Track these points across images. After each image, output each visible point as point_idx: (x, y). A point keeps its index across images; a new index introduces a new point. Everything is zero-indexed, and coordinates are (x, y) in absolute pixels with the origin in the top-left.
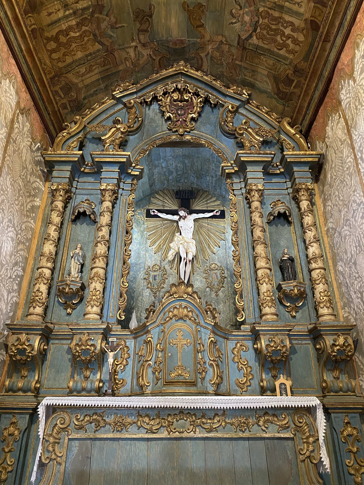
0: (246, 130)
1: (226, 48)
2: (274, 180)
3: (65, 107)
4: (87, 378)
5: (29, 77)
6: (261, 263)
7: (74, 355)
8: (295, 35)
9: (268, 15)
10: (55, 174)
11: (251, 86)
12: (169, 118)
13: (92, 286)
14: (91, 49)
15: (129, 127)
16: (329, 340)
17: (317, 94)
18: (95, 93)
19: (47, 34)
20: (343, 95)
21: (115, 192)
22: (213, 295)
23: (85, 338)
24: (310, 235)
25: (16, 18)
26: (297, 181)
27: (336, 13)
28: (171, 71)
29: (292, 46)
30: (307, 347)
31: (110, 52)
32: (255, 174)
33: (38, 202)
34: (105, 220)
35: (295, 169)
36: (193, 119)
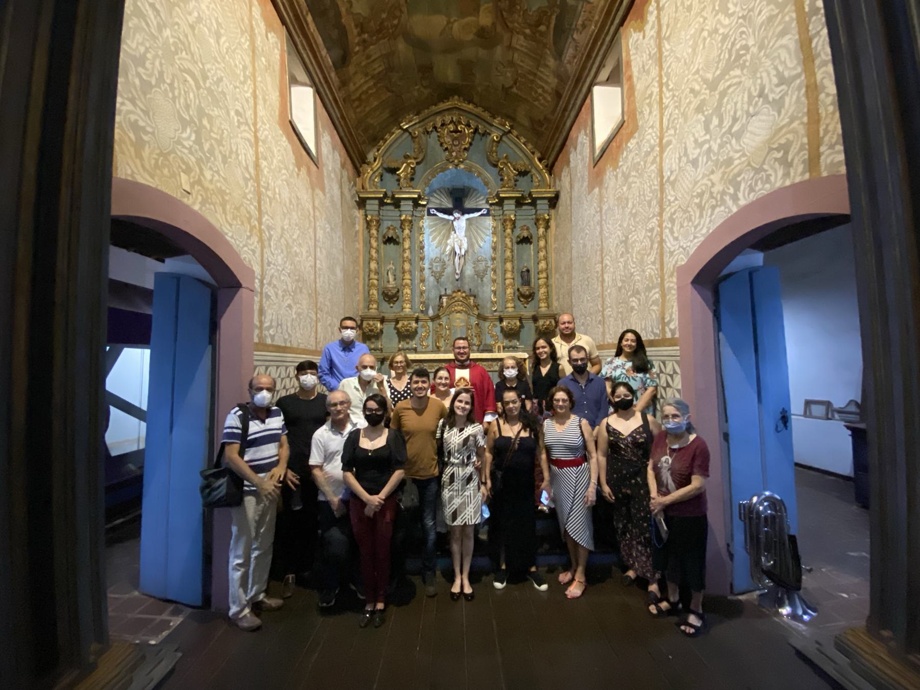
0: (506, 164)
2: (524, 207)
3: (364, 142)
5: (342, 134)
6: (509, 275)
8: (545, 95)
10: (368, 207)
11: (512, 119)
12: (446, 149)
13: (405, 291)
14: (384, 97)
15: (415, 159)
16: (541, 322)
17: (559, 143)
19: (353, 97)
20: (572, 157)
21: (411, 222)
22: (480, 281)
23: (406, 323)
24: (542, 254)
26: (539, 212)
29: (542, 101)
30: (530, 326)
34: (407, 244)
35: (538, 202)
36: (465, 149)
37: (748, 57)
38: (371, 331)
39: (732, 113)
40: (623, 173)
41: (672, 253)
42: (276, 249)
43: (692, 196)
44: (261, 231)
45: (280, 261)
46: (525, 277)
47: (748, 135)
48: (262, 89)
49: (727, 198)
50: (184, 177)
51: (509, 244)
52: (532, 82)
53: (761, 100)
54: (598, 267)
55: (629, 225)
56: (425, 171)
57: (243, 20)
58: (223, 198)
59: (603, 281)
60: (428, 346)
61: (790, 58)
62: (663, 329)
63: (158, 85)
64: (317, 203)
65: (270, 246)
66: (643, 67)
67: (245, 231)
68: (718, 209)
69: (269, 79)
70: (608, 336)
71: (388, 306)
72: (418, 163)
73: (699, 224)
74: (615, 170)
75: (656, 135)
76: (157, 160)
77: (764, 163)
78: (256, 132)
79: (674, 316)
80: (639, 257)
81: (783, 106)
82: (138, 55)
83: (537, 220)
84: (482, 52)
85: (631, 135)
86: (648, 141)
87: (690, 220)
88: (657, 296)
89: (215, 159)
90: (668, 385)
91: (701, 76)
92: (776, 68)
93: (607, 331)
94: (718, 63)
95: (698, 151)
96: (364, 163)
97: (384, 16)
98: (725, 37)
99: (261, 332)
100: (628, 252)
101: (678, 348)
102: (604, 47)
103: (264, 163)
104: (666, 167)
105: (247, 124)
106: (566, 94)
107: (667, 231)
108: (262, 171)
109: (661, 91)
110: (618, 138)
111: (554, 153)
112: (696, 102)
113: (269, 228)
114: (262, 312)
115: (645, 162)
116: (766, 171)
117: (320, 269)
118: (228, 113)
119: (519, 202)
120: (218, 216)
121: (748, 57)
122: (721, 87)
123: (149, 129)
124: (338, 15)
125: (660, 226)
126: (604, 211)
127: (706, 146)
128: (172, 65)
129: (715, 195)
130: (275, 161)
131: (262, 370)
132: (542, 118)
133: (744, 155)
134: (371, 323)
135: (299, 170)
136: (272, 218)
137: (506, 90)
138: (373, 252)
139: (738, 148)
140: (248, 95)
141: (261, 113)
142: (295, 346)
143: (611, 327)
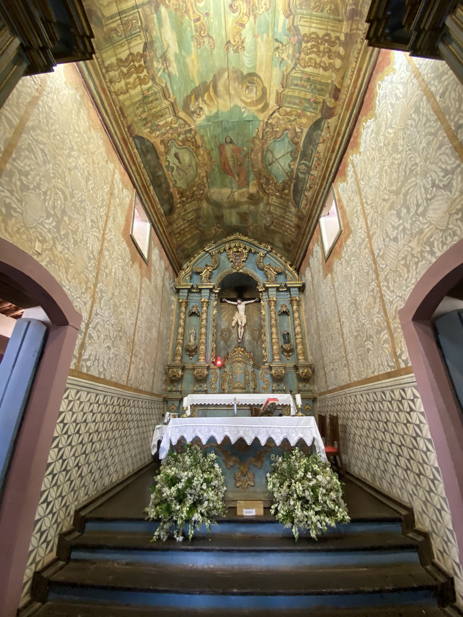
1: (259, 229)
2: (282, 293)
3: (182, 258)
4: (201, 386)
5: (168, 252)
6: (274, 336)
7: (196, 378)
9: (278, 219)
10: (180, 294)
11: (272, 244)
13: (201, 347)
14: (195, 233)
16: (301, 371)
17: (302, 255)
18: (196, 249)
19: (176, 232)
21: (208, 302)
22: (255, 343)
24: (297, 322)
25: (164, 231)
27: (307, 226)
28: (232, 237)
29: (290, 232)
31: (203, 232)
32: (272, 293)
33: (173, 307)
34: (204, 316)
35: (292, 289)
37: (419, 169)
38: (175, 376)
39: (415, 202)
40: (346, 260)
41: (391, 302)
42: (105, 306)
43: (399, 261)
44: (94, 292)
45: (106, 315)
46: (286, 337)
47: (431, 211)
48: (114, 214)
49: (426, 254)
50: (37, 244)
51: (273, 316)
52: (283, 222)
53: (434, 189)
54: (338, 325)
55: (355, 291)
56: (219, 273)
57: (107, 178)
58: (68, 264)
59: (343, 334)
60: (216, 389)
61: (449, 158)
62: (397, 361)
63: (34, 189)
64: (143, 286)
65: (100, 302)
66: (350, 199)
67: (81, 289)
68: (420, 264)
69: (119, 210)
70: (353, 375)
71: (189, 358)
72: (214, 270)
73: (408, 277)
74: (340, 259)
75: (365, 232)
76: (19, 229)
77: (448, 224)
78: (103, 235)
79: (403, 349)
80: (366, 311)
81: (453, 187)
82: (23, 170)
83: (292, 301)
84: (252, 208)
85: (348, 236)
86: (360, 237)
87: (400, 276)
88: (386, 336)
89: (68, 241)
90: (412, 410)
91: (389, 191)
92: (440, 167)
93: (351, 372)
94: (398, 179)
95: (396, 231)
96: (181, 269)
97: (195, 189)
98: (400, 164)
99: (79, 362)
100: (357, 309)
101: (413, 375)
102: (324, 196)
103: (106, 253)
104: (375, 247)
105: (98, 228)
107: (385, 288)
108: (104, 257)
109: (363, 208)
110: (339, 242)
111: (299, 261)
112: (387, 205)
113: (101, 291)
114: (83, 346)
115: (360, 249)
116: (451, 229)
117: (139, 327)
118: (85, 219)
119: (278, 289)
120: (61, 274)
121: (419, 169)
122: (403, 191)
123: (18, 210)
124: (168, 187)
125: (379, 286)
126: (336, 287)
127: (401, 227)
128: (49, 183)
129: (415, 255)
130: (115, 254)
131: (73, 392)
132: (290, 241)
133: (431, 224)
134: (175, 370)
135: (133, 263)
136: (106, 286)
137: (267, 228)
138: (182, 322)
139: (425, 221)
140: (103, 214)
141: (110, 225)
142: (108, 378)
143: (354, 368)
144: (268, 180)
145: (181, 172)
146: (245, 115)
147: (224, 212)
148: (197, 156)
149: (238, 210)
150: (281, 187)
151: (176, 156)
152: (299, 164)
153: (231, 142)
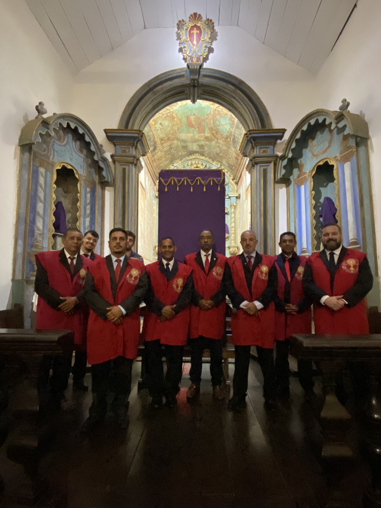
16: (231, 249)
17: (239, 176)
24: (233, 220)
25: (150, 163)
33: (154, 207)
35: (231, 198)
106: (239, 161)
132: (232, 164)
137: (218, 154)
144: (217, 133)
145: (163, 131)
146: (203, 105)
147: (188, 144)
148: (173, 122)
149: (198, 143)
150: (225, 137)
151: (161, 124)
152: (235, 130)
153: (194, 115)
